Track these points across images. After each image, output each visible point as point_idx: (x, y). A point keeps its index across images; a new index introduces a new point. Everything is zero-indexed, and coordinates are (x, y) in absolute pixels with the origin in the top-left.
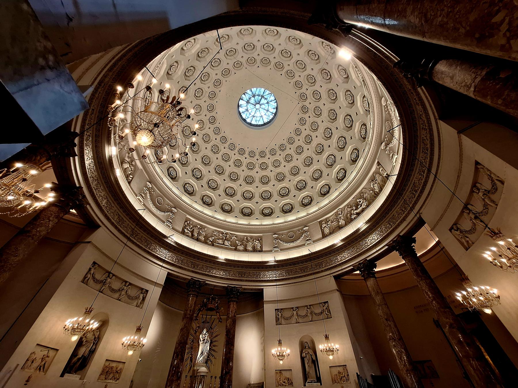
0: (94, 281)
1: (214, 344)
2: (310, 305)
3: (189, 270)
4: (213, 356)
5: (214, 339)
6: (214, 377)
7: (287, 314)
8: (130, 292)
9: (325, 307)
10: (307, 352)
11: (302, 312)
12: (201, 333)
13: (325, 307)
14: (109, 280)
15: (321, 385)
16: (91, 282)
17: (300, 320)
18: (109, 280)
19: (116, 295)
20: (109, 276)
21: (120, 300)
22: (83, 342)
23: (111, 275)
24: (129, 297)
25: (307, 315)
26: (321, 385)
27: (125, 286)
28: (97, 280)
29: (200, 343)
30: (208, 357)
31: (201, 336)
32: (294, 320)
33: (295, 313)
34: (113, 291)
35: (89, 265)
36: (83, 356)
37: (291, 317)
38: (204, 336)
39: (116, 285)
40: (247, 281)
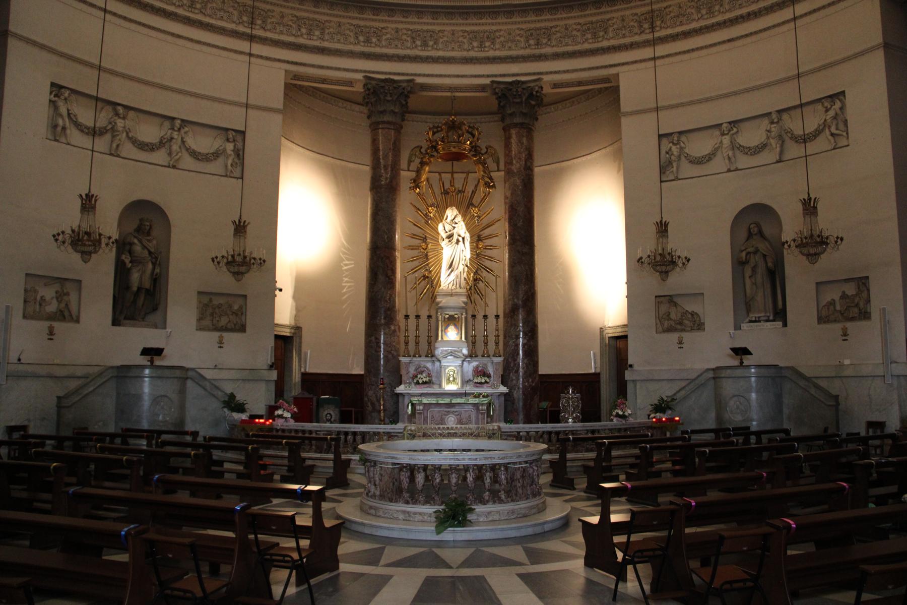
0: (82, 131)
1: (488, 242)
2: (779, 112)
3: (352, 54)
4: (486, 269)
5: (487, 232)
6: (480, 317)
7: (699, 146)
8: (191, 142)
9: (831, 113)
10: (751, 250)
11: (751, 136)
12: (441, 217)
13: (831, 113)
14: (120, 123)
15: (785, 325)
16: (75, 136)
17: (743, 161)
18: (120, 123)
19: (160, 156)
20: (117, 114)
21: (174, 167)
22: (124, 263)
23: (121, 110)
24: (194, 155)
25: (762, 147)
26: (785, 325)
27: (173, 129)
28: (88, 128)
29: (444, 244)
30: (476, 273)
31: (440, 227)
32: (719, 164)
33: (726, 140)
34: (143, 146)
35: (45, 95)
36: (139, 289)
37: (709, 158)
38: (453, 224)
39: (149, 132)
40: (557, 56)
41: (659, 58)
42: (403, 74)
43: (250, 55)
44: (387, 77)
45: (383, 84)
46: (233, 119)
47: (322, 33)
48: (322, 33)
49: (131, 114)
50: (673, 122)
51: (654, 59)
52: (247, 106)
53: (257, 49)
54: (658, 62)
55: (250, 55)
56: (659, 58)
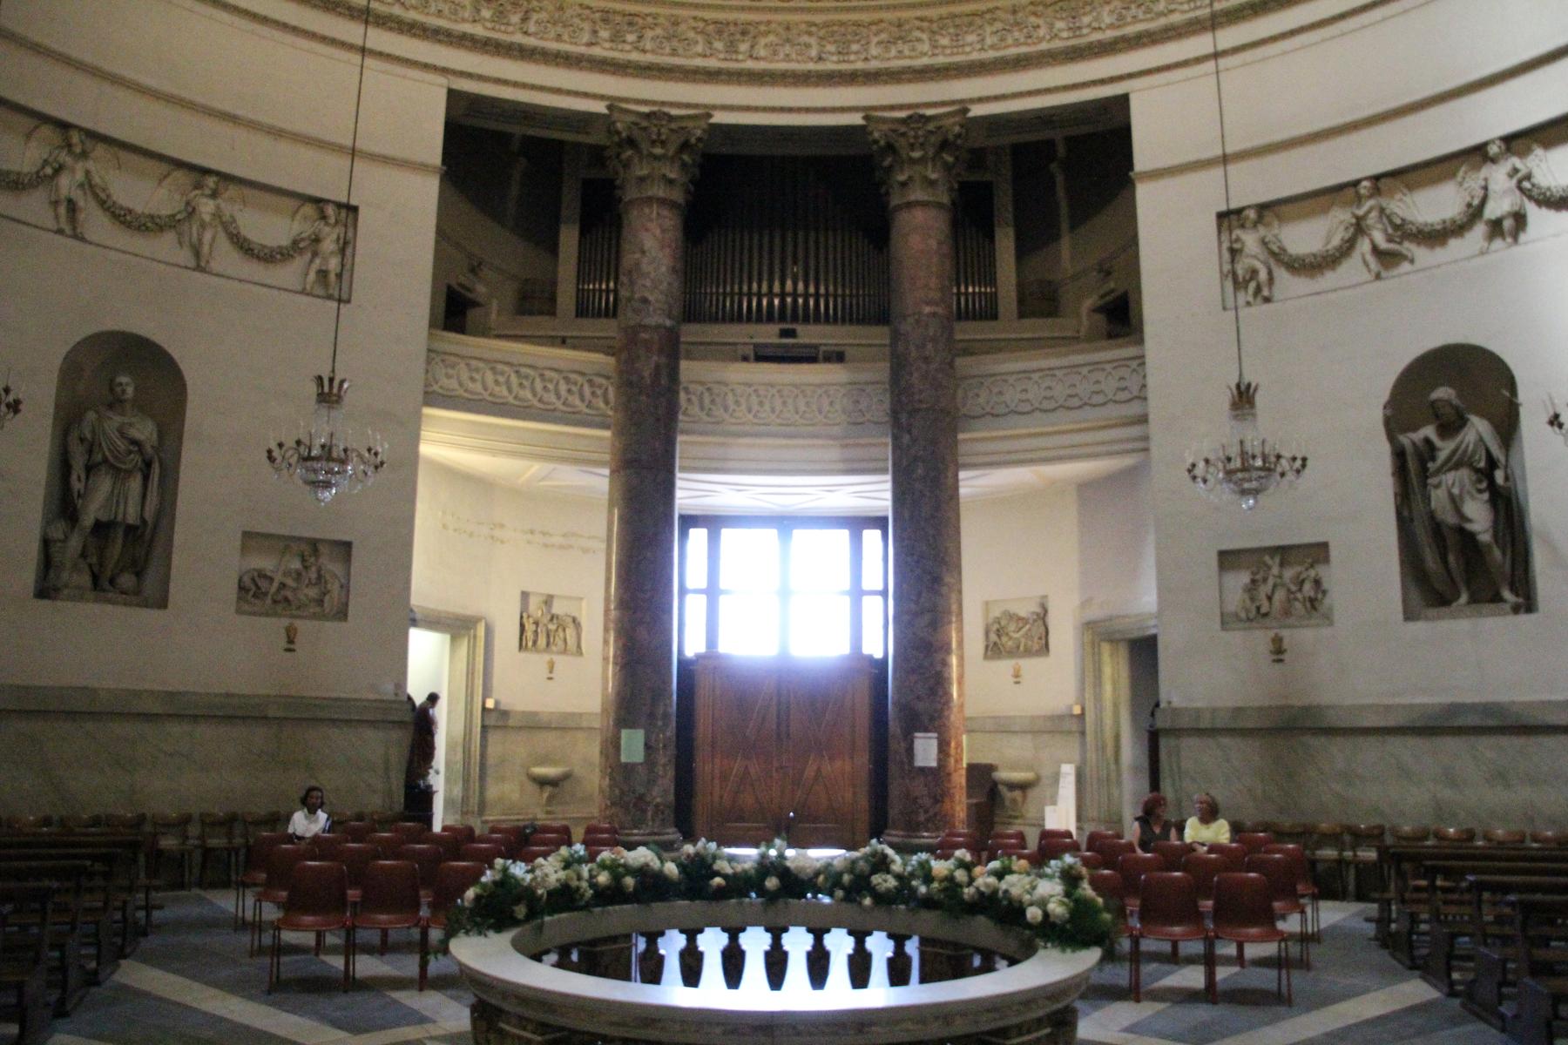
41: (1225, 53)
42: (688, 106)
43: (363, 51)
44: (655, 109)
45: (645, 124)
46: (322, 176)
47: (525, 20)
48: (525, 20)
49: (100, 150)
50: (1254, 184)
51: (1216, 55)
52: (353, 152)
53: (379, 39)
54: (1223, 62)
55: (363, 51)
56: (1225, 53)
